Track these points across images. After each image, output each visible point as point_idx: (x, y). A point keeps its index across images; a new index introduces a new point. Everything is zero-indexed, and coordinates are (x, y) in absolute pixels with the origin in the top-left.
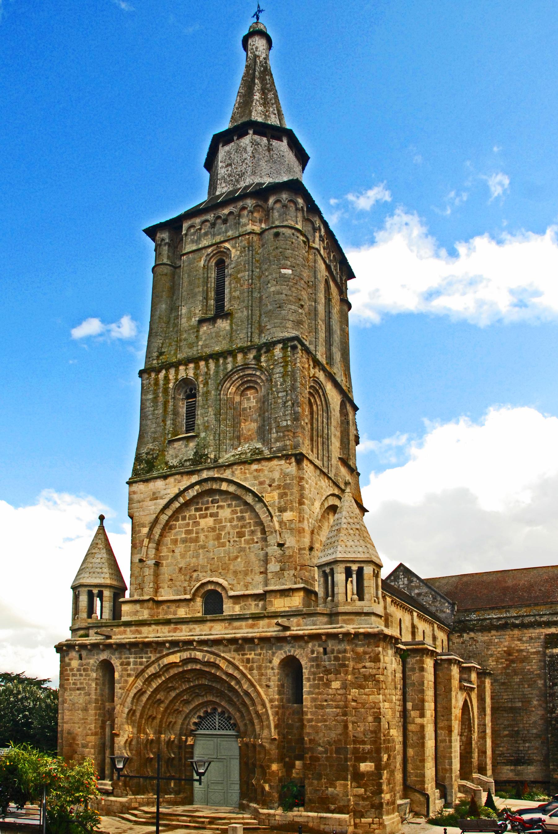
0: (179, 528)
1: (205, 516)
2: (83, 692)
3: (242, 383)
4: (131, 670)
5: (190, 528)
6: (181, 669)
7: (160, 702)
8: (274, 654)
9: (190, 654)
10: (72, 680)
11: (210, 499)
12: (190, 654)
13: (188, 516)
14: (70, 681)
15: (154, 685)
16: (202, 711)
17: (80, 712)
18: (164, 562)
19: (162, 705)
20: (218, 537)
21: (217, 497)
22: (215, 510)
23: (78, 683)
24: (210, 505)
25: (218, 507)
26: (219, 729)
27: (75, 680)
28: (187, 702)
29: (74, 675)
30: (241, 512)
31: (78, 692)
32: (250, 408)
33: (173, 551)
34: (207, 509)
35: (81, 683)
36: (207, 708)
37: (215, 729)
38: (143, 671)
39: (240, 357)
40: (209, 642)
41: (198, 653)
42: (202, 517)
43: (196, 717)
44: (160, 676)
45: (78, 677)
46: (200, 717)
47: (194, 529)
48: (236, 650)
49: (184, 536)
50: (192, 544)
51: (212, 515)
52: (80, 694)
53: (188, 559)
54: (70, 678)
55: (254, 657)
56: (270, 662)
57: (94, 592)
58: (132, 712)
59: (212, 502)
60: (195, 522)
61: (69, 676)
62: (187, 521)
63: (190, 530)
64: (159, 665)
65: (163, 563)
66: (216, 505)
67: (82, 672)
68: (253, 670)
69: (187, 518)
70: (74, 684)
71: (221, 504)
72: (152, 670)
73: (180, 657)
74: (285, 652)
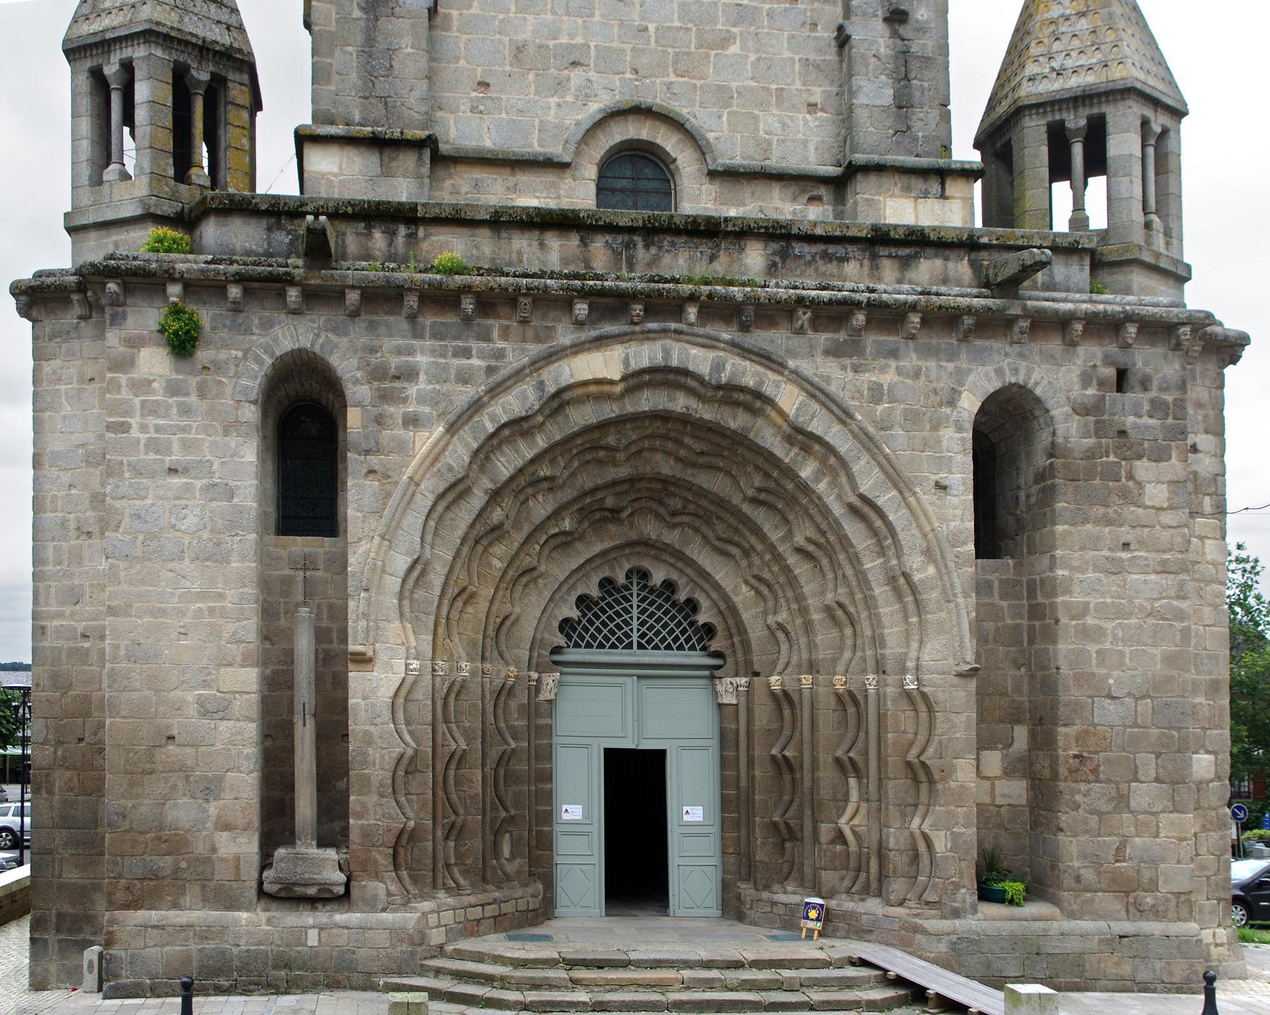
2: (199, 484)
4: (421, 399)
6: (610, 411)
7: (497, 532)
8: (960, 376)
9: (667, 353)
10: (144, 428)
12: (667, 353)
14: (135, 433)
15: (506, 464)
16: (596, 580)
17: (187, 565)
19: (500, 549)
23: (176, 446)
26: (640, 646)
27: (158, 429)
28: (565, 542)
29: (150, 409)
31: (177, 481)
35: (187, 446)
36: (612, 568)
37: (630, 646)
38: (476, 406)
40: (750, 311)
41: (694, 351)
43: (573, 599)
44: (527, 434)
45: (174, 420)
46: (582, 601)
48: (834, 352)
52: (187, 488)
53: (549, 17)
54: (135, 421)
55: (896, 378)
56: (952, 403)
58: (418, 569)
61: (128, 413)
64: (541, 385)
65: (447, 17)
67: (193, 399)
68: (891, 428)
70: (152, 445)
72: (512, 404)
73: (626, 362)
74: (999, 372)
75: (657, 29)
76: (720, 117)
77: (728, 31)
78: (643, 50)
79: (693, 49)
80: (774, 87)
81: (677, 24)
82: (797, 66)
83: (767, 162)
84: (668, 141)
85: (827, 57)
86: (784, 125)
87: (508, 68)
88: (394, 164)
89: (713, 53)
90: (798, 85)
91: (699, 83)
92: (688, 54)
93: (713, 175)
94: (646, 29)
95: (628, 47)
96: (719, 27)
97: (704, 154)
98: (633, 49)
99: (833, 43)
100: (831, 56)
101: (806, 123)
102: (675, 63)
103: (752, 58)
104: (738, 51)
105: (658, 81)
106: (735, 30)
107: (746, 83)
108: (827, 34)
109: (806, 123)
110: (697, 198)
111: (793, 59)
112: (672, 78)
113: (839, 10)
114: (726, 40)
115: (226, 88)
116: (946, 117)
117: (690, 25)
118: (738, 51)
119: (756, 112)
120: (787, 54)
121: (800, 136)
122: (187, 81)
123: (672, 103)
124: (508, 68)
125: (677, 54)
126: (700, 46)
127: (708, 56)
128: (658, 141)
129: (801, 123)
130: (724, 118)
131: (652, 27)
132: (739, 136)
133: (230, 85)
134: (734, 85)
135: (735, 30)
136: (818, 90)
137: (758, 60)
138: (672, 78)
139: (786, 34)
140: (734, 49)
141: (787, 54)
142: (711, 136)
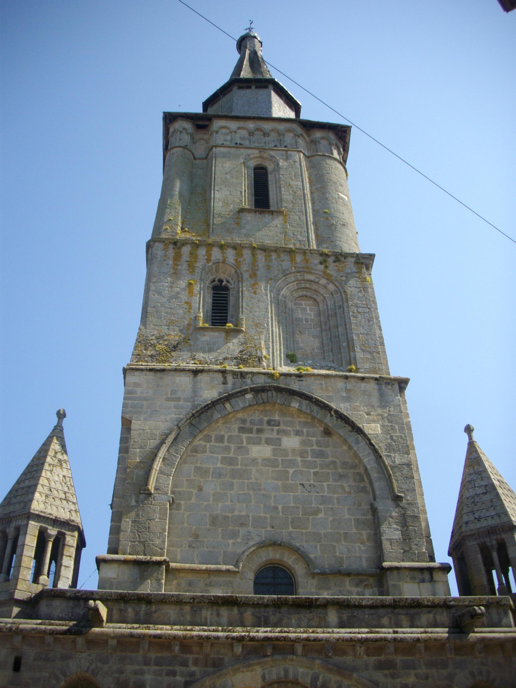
0: (211, 452)
1: (258, 442)
3: (298, 289)
5: (231, 455)
11: (266, 419)
13: (226, 437)
18: (183, 502)
20: (284, 475)
21: (277, 418)
22: (274, 435)
24: (265, 426)
25: (278, 432)
30: (318, 443)
32: (307, 320)
33: (200, 489)
34: (259, 431)
39: (299, 258)
42: (250, 441)
47: (239, 457)
49: (219, 465)
50: (235, 481)
51: (268, 442)
57: (49, 531)
59: (269, 423)
60: (239, 448)
62: (226, 444)
63: (231, 458)
66: (276, 428)
69: (226, 440)
71: (282, 427)
75: (283, 508)
76: (316, 547)
77: (318, 507)
78: (276, 517)
79: (301, 515)
80: (342, 532)
81: (292, 505)
82: (353, 523)
83: (342, 568)
84: (290, 560)
85: (367, 517)
86: (349, 550)
87: (208, 526)
88: (146, 573)
89: (311, 517)
90: (354, 530)
91: (304, 531)
92: (299, 518)
93: (313, 575)
94: (277, 508)
95: (268, 516)
96: (313, 505)
97: (308, 565)
98: (271, 517)
99: (370, 511)
100: (370, 517)
101: (360, 549)
102: (292, 523)
103: (330, 519)
104: (323, 516)
105: (284, 531)
106: (321, 507)
107: (328, 531)
108: (366, 507)
109: (360, 549)
110: (307, 589)
111: (351, 519)
112: (291, 529)
113: (371, 496)
114: (317, 512)
115: (65, 538)
116: (430, 542)
117: (298, 505)
118: (323, 516)
119: (335, 544)
120: (347, 516)
121: (357, 555)
122: (45, 535)
123: (291, 541)
124: (208, 526)
125: (293, 519)
126: (304, 514)
127: (308, 519)
128: (285, 559)
129: (357, 548)
130: (318, 547)
131: (280, 507)
132: (326, 555)
133: (66, 536)
134: (322, 532)
135: (321, 507)
136: (364, 532)
137: (334, 520)
138: (291, 529)
139: (346, 508)
140: (321, 515)
141: (347, 516)
142: (312, 556)
